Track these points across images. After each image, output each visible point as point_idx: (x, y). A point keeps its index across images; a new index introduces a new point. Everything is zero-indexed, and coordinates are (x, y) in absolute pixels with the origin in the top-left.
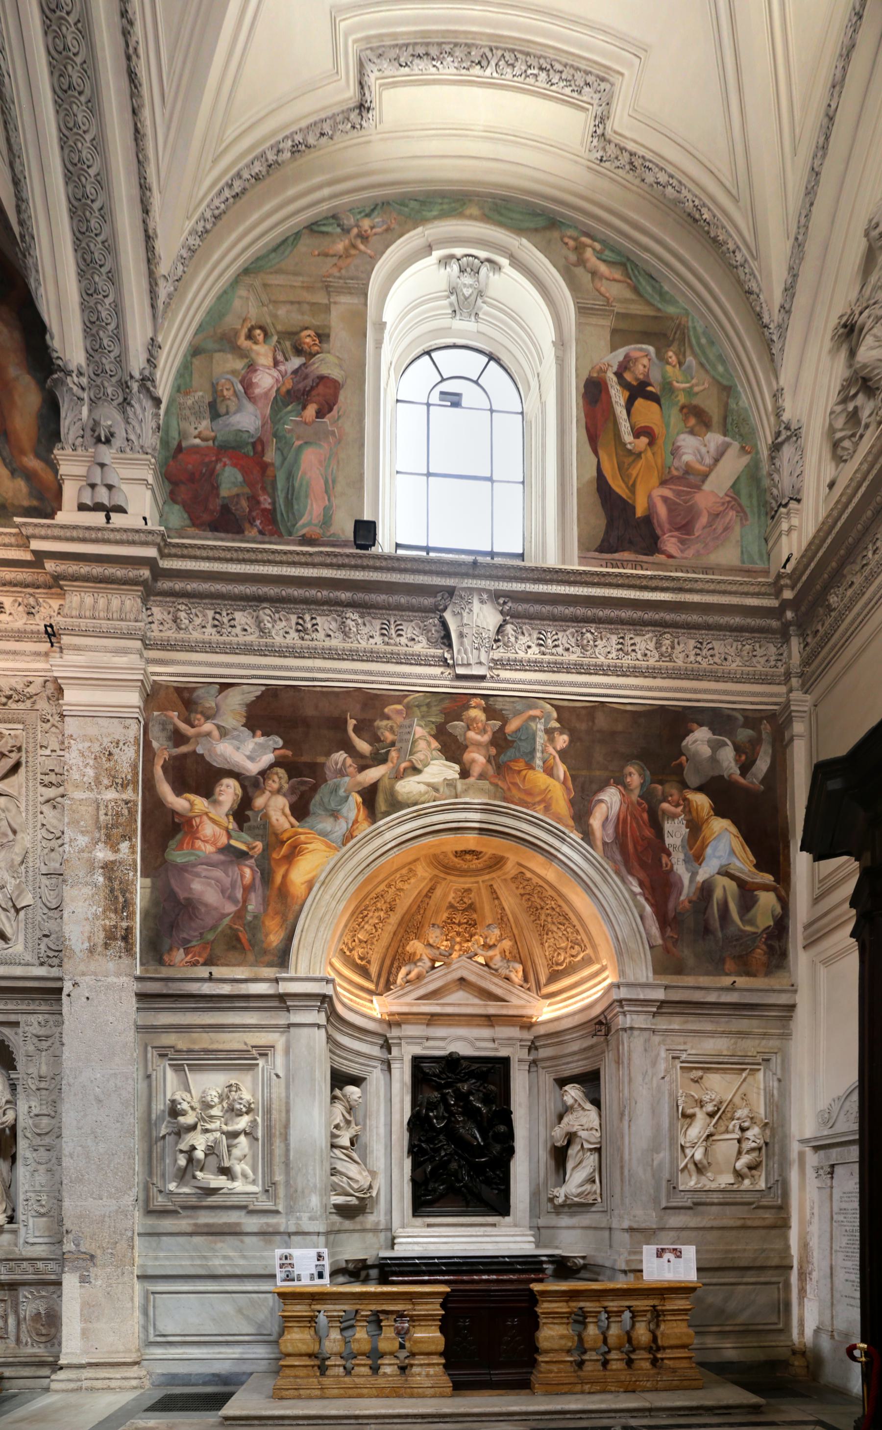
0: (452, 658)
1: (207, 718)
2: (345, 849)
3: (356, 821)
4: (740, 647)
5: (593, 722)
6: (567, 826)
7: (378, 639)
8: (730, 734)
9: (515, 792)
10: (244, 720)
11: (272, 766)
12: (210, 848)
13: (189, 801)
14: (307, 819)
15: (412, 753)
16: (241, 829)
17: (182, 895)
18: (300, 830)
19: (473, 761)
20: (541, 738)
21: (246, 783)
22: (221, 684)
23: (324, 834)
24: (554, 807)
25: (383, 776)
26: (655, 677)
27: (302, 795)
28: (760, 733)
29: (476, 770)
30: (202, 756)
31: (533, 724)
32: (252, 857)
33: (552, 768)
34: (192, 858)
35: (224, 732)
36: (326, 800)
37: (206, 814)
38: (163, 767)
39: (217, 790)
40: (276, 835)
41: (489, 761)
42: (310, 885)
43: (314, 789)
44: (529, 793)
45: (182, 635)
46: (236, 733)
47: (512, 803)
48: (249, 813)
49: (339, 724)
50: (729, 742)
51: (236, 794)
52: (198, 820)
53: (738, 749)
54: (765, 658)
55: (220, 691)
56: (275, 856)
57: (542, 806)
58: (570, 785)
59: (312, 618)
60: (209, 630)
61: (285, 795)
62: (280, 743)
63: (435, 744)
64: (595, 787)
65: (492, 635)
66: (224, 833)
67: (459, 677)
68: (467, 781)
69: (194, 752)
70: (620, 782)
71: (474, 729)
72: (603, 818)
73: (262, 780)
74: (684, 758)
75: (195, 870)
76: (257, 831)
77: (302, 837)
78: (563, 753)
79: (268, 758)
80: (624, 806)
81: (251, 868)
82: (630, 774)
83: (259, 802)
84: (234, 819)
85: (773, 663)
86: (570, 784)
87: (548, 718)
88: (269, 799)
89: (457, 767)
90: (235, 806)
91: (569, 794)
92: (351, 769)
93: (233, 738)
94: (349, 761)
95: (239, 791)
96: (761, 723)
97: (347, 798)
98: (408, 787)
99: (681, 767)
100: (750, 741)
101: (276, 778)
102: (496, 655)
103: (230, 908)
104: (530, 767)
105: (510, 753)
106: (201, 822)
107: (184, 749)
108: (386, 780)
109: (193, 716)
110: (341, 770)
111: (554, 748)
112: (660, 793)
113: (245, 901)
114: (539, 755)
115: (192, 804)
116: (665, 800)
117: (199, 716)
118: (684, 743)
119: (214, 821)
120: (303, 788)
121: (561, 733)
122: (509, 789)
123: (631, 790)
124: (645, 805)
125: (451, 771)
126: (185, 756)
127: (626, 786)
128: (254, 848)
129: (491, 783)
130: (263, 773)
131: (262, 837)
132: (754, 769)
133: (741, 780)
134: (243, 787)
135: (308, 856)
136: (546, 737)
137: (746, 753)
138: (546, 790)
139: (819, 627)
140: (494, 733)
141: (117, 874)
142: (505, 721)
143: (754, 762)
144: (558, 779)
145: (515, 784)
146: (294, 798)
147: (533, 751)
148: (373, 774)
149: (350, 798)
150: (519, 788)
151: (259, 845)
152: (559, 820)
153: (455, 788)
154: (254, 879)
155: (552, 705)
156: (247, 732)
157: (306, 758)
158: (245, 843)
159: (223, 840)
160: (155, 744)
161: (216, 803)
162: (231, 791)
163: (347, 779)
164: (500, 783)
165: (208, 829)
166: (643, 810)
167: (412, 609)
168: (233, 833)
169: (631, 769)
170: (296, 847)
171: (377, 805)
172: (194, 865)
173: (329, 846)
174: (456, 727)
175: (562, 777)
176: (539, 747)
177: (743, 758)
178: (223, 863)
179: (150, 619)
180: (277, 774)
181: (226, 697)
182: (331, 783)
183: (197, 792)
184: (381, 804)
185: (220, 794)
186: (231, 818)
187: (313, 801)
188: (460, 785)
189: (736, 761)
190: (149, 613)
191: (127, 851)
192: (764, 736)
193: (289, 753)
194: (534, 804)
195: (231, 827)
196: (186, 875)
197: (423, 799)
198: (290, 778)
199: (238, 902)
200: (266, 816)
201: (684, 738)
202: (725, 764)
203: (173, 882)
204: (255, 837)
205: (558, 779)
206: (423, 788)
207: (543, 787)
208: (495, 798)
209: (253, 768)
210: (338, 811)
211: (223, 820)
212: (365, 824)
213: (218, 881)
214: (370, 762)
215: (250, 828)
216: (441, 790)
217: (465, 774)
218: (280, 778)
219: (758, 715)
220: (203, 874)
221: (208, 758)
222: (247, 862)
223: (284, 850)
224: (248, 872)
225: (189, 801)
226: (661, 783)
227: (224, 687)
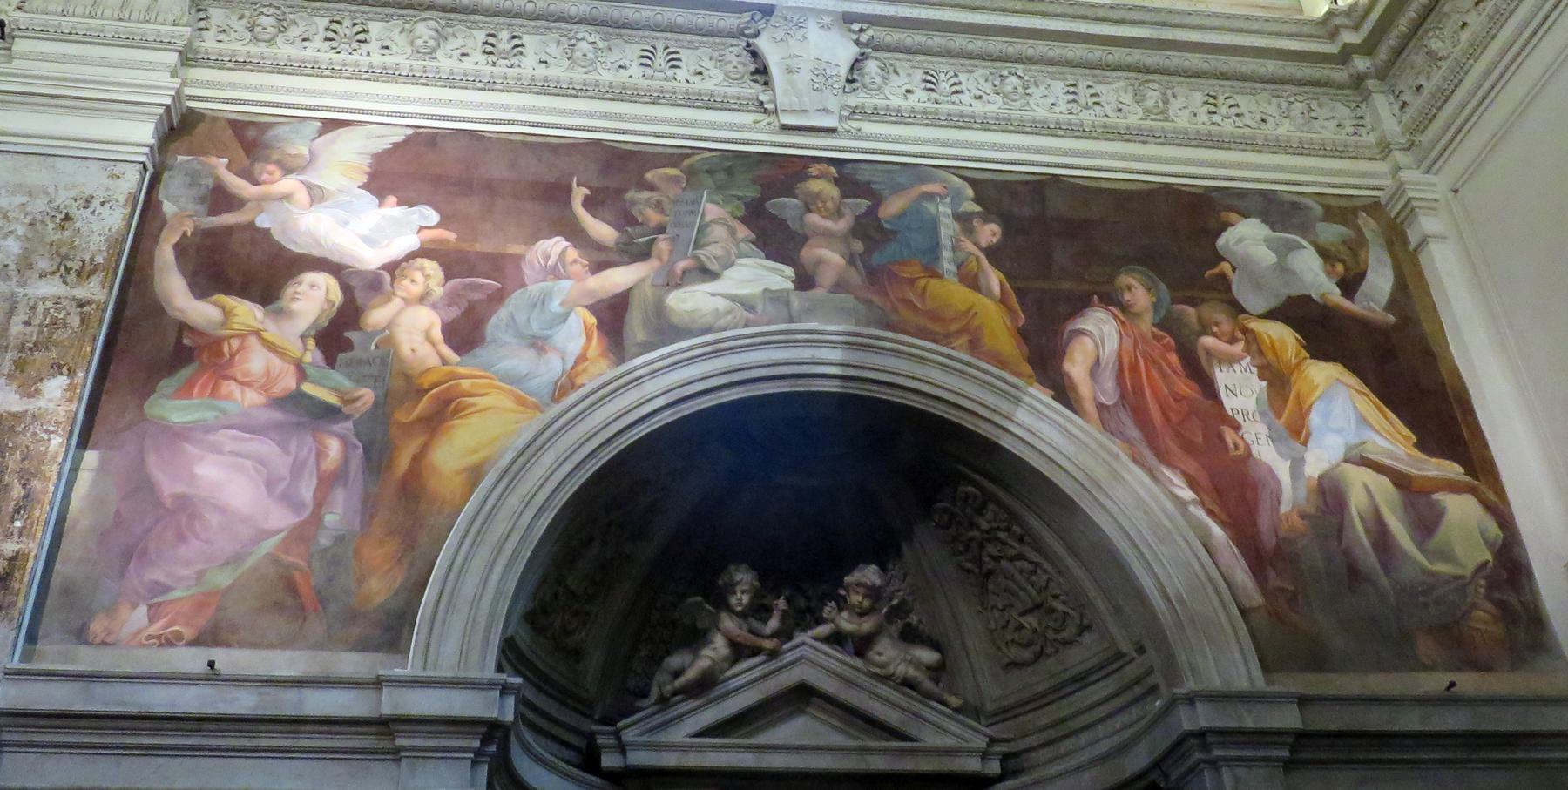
0: (774, 101)
1: (288, 171)
2: (557, 409)
3: (582, 358)
4: (1284, 105)
5: (1043, 200)
6: (1018, 375)
7: (635, 70)
8: (1305, 229)
9: (906, 314)
10: (364, 179)
11: (412, 256)
12: (253, 397)
13: (223, 308)
14: (477, 351)
15: (697, 245)
16: (331, 362)
17: (169, 487)
18: (462, 370)
19: (820, 262)
20: (948, 229)
21: (354, 282)
22: (324, 121)
23: (513, 380)
24: (987, 342)
25: (643, 280)
26: (1145, 142)
27: (470, 310)
28: (1359, 231)
29: (827, 277)
30: (266, 232)
31: (930, 207)
32: (348, 417)
33: (976, 277)
34: (209, 415)
35: (317, 195)
36: (521, 318)
37: (257, 333)
38: (176, 247)
39: (289, 291)
40: (407, 377)
41: (851, 260)
42: (475, 475)
43: (498, 298)
44: (934, 316)
45: (261, 48)
46: (343, 198)
47: (904, 332)
48: (353, 335)
49: (556, 193)
50: (1305, 243)
51: (328, 301)
52: (235, 344)
53: (1325, 254)
54: (1335, 122)
55: (321, 133)
56: (402, 416)
57: (964, 340)
58: (1017, 306)
59: (514, 37)
60: (317, 43)
61: (434, 306)
62: (433, 217)
63: (743, 232)
64: (1063, 309)
65: (844, 71)
66: (292, 367)
67: (786, 128)
68: (810, 293)
69: (251, 226)
70: (1111, 300)
71: (819, 211)
72: (1090, 362)
73: (387, 277)
74: (1225, 267)
75: (211, 438)
76: (366, 370)
77: (465, 384)
78: (993, 254)
79: (411, 242)
80: (1128, 343)
81: (344, 439)
82: (1129, 288)
83: (377, 316)
84: (317, 344)
85: (1351, 130)
86: (1013, 300)
87: (957, 196)
88: (399, 313)
89: (789, 271)
90: (325, 322)
91: (1014, 318)
92: (577, 267)
93: (337, 206)
94: (573, 254)
95: (337, 296)
96: (1356, 217)
97: (564, 317)
98: (692, 300)
99: (1223, 283)
100: (1344, 242)
101: (418, 276)
102: (853, 100)
103: (281, 519)
104: (935, 274)
105: (891, 250)
106: (241, 348)
107: (229, 219)
108: (648, 290)
109: (258, 167)
110: (554, 270)
111: (977, 245)
112: (1194, 319)
113: (320, 504)
114: (947, 254)
115: (227, 313)
116: (1205, 330)
117: (271, 168)
118: (1221, 242)
119: (271, 347)
120: (476, 296)
121: (986, 221)
122: (895, 310)
123: (1137, 315)
124: (1169, 340)
125: (780, 277)
126: (229, 230)
127: (1124, 308)
128: (355, 400)
129: (857, 298)
130: (393, 268)
131: (376, 381)
132: (1364, 287)
133: (1346, 303)
134: (346, 289)
135: (474, 420)
136: (957, 226)
137: (1343, 261)
138: (969, 314)
139: (1422, 81)
140: (857, 218)
141: (20, 439)
142: (877, 199)
143: (1361, 276)
144: (989, 294)
145: (908, 303)
146: (454, 313)
147: (938, 244)
148: (619, 278)
149: (572, 317)
150: (915, 308)
151: (367, 395)
152: (1001, 363)
153: (788, 304)
154: (346, 460)
155: (964, 178)
156: (368, 198)
157: (485, 246)
158: (334, 389)
159: (289, 382)
160: (168, 208)
161: (282, 314)
162: (319, 295)
163: (566, 284)
164: (876, 299)
165: (256, 361)
166: (1167, 347)
167: (699, 32)
168: (310, 371)
169: (1125, 279)
170: (448, 402)
171: (627, 330)
172: (209, 429)
173: (521, 402)
174: (785, 207)
175: (996, 289)
176: (945, 241)
177: (1340, 268)
178: (279, 427)
179: (202, 25)
180: (422, 269)
181: (333, 141)
182: (533, 289)
183: (243, 292)
184: (636, 328)
185: (293, 299)
186: (311, 343)
187: (494, 320)
188: (797, 301)
189: (1329, 274)
190: (202, 15)
191: (58, 394)
192: (1368, 235)
193: (451, 236)
194: (948, 336)
195: (308, 358)
196: (189, 447)
197: (722, 322)
198: (448, 276)
199: (304, 505)
200: (388, 344)
201: (1219, 234)
202: (1308, 278)
203: (152, 460)
204: (359, 381)
205: (989, 294)
206: (722, 304)
207: (963, 308)
208: (868, 325)
209: (370, 258)
210: (547, 338)
211: (295, 348)
212: (603, 365)
213: (261, 461)
214: (614, 257)
215: (349, 364)
216: (760, 308)
217: (805, 281)
218: (427, 277)
219: (1344, 203)
220: (230, 446)
221: (277, 236)
222: (337, 428)
223: (423, 405)
224: (334, 447)
225: (223, 308)
226: (1192, 302)
227: (330, 125)
